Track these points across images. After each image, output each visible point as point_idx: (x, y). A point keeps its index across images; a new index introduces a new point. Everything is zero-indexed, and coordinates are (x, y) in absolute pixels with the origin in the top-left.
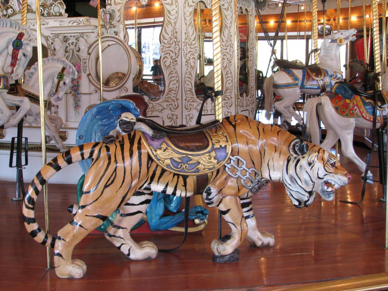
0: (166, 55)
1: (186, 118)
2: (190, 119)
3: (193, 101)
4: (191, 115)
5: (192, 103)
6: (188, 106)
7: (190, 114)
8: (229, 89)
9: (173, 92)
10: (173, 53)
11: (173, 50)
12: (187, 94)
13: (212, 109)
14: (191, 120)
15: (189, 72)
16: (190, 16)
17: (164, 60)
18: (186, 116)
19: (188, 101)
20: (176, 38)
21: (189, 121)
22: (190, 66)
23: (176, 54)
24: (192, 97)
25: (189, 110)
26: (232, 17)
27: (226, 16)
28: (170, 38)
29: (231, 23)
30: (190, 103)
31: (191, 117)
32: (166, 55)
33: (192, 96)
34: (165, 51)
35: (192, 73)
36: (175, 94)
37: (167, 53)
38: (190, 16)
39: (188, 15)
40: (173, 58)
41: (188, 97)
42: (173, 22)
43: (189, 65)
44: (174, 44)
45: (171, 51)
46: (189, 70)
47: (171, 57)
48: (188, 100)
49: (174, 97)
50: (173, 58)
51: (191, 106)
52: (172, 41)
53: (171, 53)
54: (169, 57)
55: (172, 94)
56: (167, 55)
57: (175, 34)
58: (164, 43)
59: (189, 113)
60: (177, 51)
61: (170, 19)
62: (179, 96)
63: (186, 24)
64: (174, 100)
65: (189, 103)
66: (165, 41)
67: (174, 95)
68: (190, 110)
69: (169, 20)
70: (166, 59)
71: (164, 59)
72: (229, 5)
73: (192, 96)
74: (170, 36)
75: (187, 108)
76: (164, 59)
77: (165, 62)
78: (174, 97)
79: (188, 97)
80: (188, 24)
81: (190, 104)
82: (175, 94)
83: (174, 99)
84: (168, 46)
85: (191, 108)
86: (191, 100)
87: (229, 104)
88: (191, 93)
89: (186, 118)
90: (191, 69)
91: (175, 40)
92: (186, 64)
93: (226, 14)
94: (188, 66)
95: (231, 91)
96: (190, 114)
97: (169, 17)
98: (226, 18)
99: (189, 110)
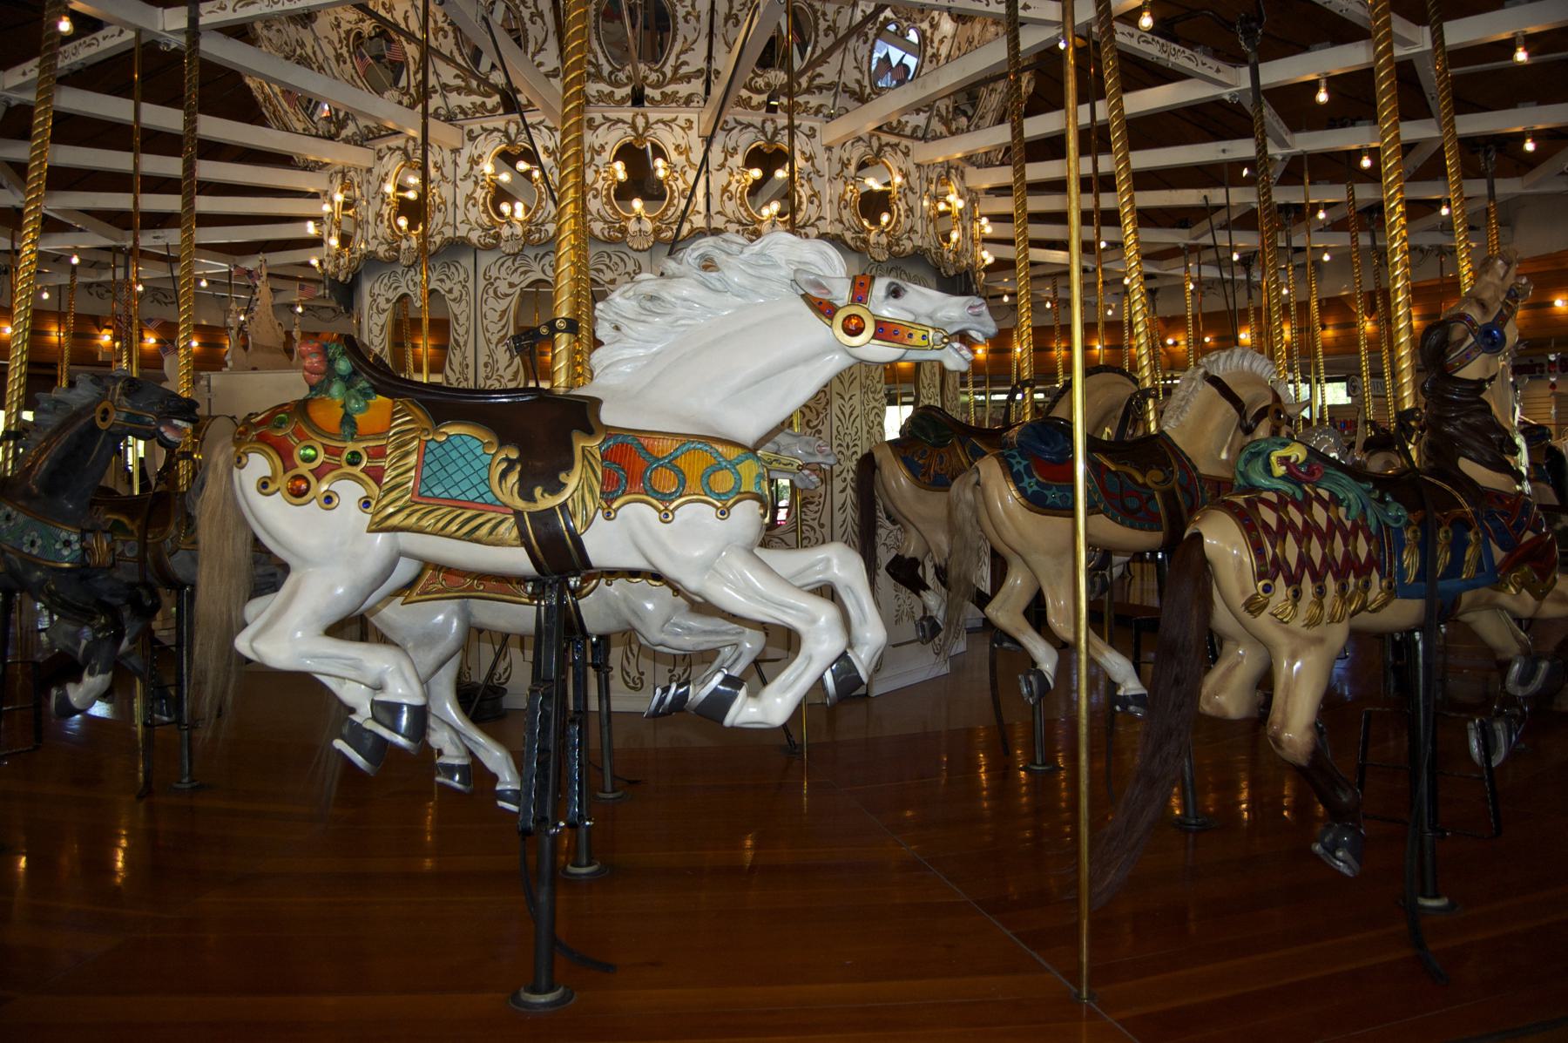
8: (812, 503)
9: (812, 507)
10: (811, 411)
23: (818, 415)
27: (455, 316)
36: (816, 512)
40: (811, 425)
49: (814, 519)
50: (811, 425)
55: (808, 513)
60: (820, 408)
62: (825, 520)
63: (488, 341)
64: (813, 528)
67: (814, 516)
72: (464, 287)
78: (814, 519)
80: (494, 341)
82: (816, 512)
83: (815, 524)
93: (457, 313)
95: (821, 507)
98: (457, 319)
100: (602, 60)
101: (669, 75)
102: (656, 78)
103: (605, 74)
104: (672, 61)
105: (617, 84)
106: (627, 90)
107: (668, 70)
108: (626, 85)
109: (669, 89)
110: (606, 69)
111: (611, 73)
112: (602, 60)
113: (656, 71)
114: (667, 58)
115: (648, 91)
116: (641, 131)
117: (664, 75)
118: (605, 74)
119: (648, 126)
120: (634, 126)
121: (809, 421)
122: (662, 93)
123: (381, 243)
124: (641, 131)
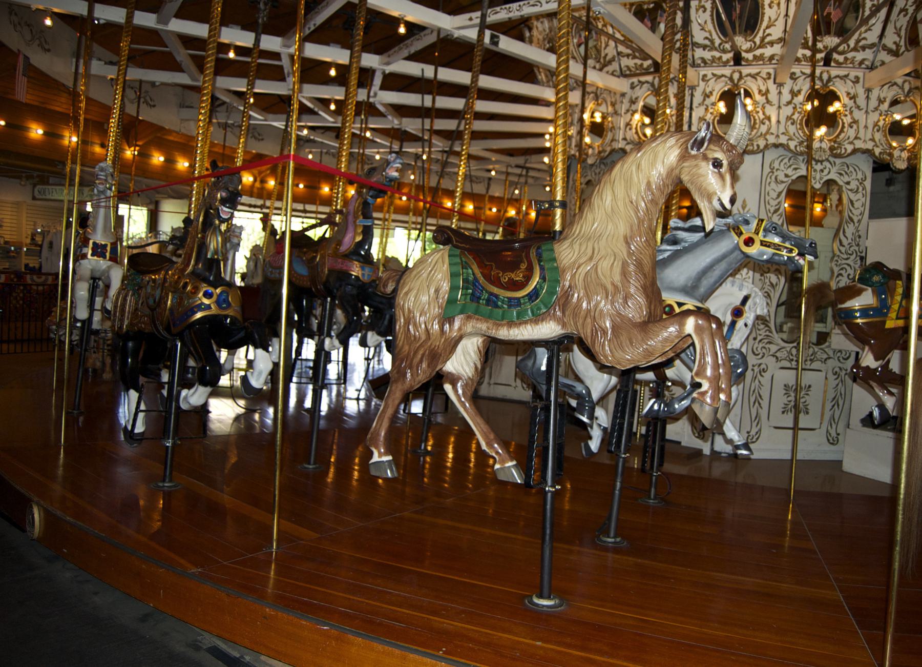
0: (841, 272)
1: (753, 370)
2: (760, 372)
3: (770, 343)
4: (763, 366)
5: (767, 346)
6: (759, 349)
7: (760, 365)
11: (852, 264)
12: (759, 330)
13: (808, 358)
14: (763, 374)
15: (766, 292)
16: (777, 198)
17: (838, 279)
18: (753, 366)
19: (760, 341)
20: (858, 245)
21: (758, 375)
22: (768, 283)
24: (767, 336)
25: (760, 356)
26: (863, 205)
28: (849, 244)
29: (862, 214)
30: (764, 345)
31: (763, 369)
32: (841, 272)
33: (767, 333)
34: (840, 265)
35: (772, 295)
37: (842, 269)
38: (777, 198)
39: (775, 196)
40: (851, 277)
41: (760, 335)
42: (856, 219)
43: (767, 281)
44: (854, 255)
45: (848, 265)
46: (766, 290)
47: (849, 275)
48: (759, 338)
51: (764, 350)
52: (852, 249)
53: (848, 268)
54: (845, 275)
56: (843, 272)
57: (858, 239)
58: (840, 251)
59: (760, 361)
61: (853, 214)
65: (761, 345)
66: (841, 248)
68: (763, 357)
69: (851, 215)
70: (840, 277)
71: (837, 277)
73: (767, 333)
74: (850, 241)
75: (757, 353)
76: (837, 277)
77: (838, 282)
79: (760, 335)
81: (764, 348)
84: (845, 256)
85: (764, 353)
86: (766, 341)
87: (843, 355)
88: (767, 328)
89: (753, 370)
90: (769, 288)
91: (857, 248)
92: (760, 280)
94: (764, 283)
96: (760, 365)
97: (851, 211)
99: (760, 356)
100: (715, 36)
101: (758, 43)
102: (749, 46)
103: (717, 45)
104: (760, 34)
105: (724, 51)
106: (731, 55)
107: (757, 40)
108: (730, 52)
109: (758, 52)
110: (717, 42)
111: (720, 45)
112: (715, 36)
113: (750, 41)
114: (758, 32)
115: (744, 55)
116: (736, 82)
117: (755, 43)
118: (717, 45)
119: (741, 78)
120: (731, 79)
121: (849, 275)
122: (754, 55)
123: (628, 143)
124: (736, 82)
